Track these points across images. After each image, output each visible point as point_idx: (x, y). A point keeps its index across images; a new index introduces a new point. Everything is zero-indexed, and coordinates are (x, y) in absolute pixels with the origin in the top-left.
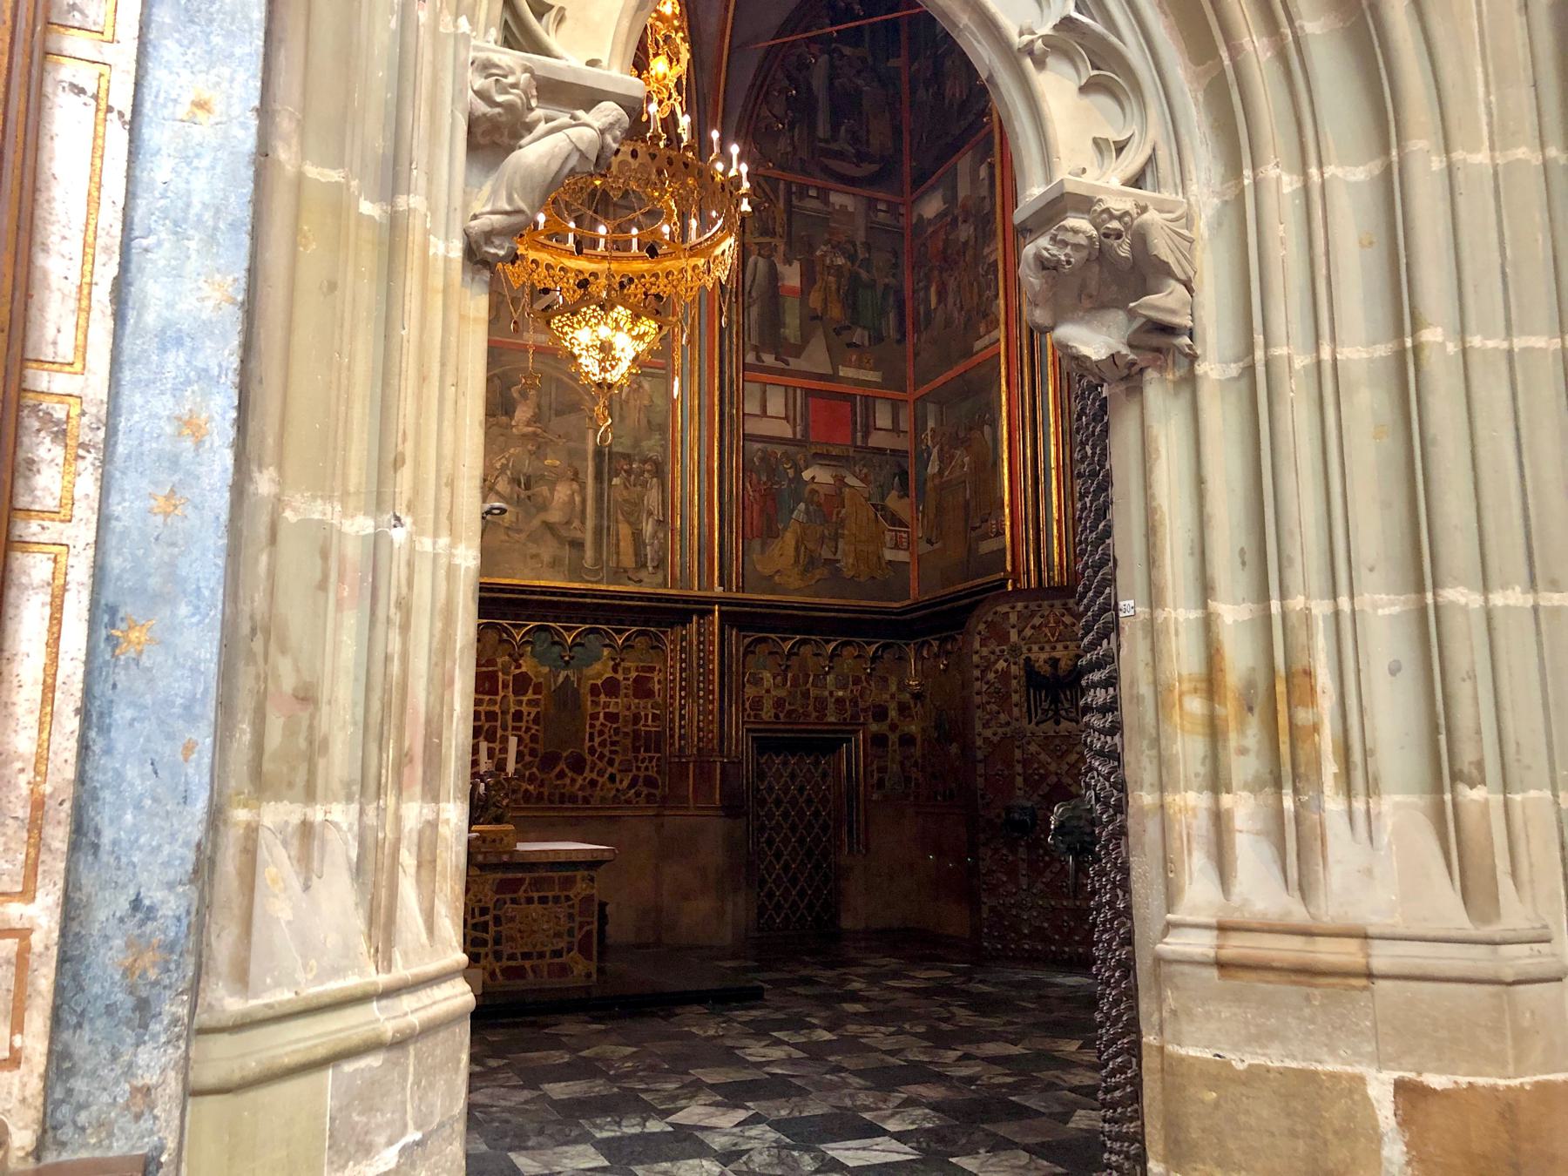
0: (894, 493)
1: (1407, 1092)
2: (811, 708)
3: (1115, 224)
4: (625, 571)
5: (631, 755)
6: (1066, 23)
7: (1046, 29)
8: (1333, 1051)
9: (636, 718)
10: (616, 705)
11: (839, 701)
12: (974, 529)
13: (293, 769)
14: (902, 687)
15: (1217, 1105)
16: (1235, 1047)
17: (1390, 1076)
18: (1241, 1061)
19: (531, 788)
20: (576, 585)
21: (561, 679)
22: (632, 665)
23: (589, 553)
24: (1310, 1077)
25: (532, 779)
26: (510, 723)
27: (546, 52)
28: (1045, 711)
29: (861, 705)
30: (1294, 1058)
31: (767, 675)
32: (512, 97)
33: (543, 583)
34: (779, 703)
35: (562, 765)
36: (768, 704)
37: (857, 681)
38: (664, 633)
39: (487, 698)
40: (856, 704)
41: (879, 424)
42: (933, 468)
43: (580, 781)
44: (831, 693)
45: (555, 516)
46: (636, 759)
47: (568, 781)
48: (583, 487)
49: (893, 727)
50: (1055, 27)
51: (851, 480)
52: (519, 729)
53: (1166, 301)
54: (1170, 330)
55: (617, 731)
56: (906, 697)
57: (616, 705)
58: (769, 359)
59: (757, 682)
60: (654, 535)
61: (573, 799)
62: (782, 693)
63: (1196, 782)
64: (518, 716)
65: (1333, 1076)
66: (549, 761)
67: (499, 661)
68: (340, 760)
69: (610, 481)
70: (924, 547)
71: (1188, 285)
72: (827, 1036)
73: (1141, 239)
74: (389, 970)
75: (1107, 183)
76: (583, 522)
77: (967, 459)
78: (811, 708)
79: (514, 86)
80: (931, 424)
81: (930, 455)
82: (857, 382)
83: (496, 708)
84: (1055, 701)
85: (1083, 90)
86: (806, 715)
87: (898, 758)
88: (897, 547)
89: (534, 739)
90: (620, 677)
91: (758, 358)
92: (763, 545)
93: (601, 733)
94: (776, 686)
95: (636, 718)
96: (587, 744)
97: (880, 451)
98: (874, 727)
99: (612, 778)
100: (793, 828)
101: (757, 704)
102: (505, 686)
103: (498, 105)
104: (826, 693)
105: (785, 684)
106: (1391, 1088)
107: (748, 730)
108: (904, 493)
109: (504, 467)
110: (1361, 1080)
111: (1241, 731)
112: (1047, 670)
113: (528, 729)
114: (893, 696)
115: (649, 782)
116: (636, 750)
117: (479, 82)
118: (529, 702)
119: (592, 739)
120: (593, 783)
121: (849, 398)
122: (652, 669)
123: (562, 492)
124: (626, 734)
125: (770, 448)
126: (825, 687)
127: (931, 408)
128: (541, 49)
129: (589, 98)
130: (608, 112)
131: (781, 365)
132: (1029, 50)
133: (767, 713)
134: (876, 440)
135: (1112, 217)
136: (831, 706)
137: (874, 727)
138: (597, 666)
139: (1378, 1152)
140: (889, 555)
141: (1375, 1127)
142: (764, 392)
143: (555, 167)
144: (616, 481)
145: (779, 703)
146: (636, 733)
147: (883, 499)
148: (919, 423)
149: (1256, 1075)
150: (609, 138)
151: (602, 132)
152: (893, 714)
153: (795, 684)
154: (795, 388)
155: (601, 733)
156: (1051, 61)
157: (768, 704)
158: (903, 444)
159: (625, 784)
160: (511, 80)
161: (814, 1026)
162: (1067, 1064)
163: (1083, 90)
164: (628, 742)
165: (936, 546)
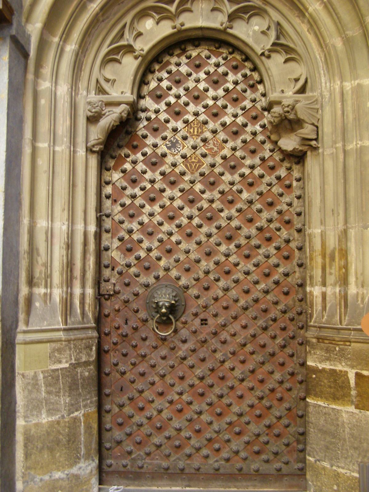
1: (358, 375)
3: (286, 109)
6: (274, 44)
7: (269, 47)
8: (341, 363)
13: (42, 281)
15: (315, 378)
16: (320, 362)
17: (354, 371)
18: (320, 366)
24: (334, 371)
27: (108, 94)
30: (331, 365)
32: (97, 109)
50: (271, 46)
53: (307, 131)
63: (319, 283)
65: (341, 371)
68: (57, 278)
71: (313, 124)
74: (67, 325)
79: (97, 106)
85: (286, 61)
106: (354, 375)
110: (346, 372)
111: (331, 268)
117: (89, 107)
129: (118, 104)
130: (123, 107)
132: (263, 54)
135: (286, 107)
139: (350, 393)
141: (350, 386)
143: (107, 126)
149: (324, 369)
150: (123, 114)
151: (121, 113)
160: (96, 105)
163: (286, 61)
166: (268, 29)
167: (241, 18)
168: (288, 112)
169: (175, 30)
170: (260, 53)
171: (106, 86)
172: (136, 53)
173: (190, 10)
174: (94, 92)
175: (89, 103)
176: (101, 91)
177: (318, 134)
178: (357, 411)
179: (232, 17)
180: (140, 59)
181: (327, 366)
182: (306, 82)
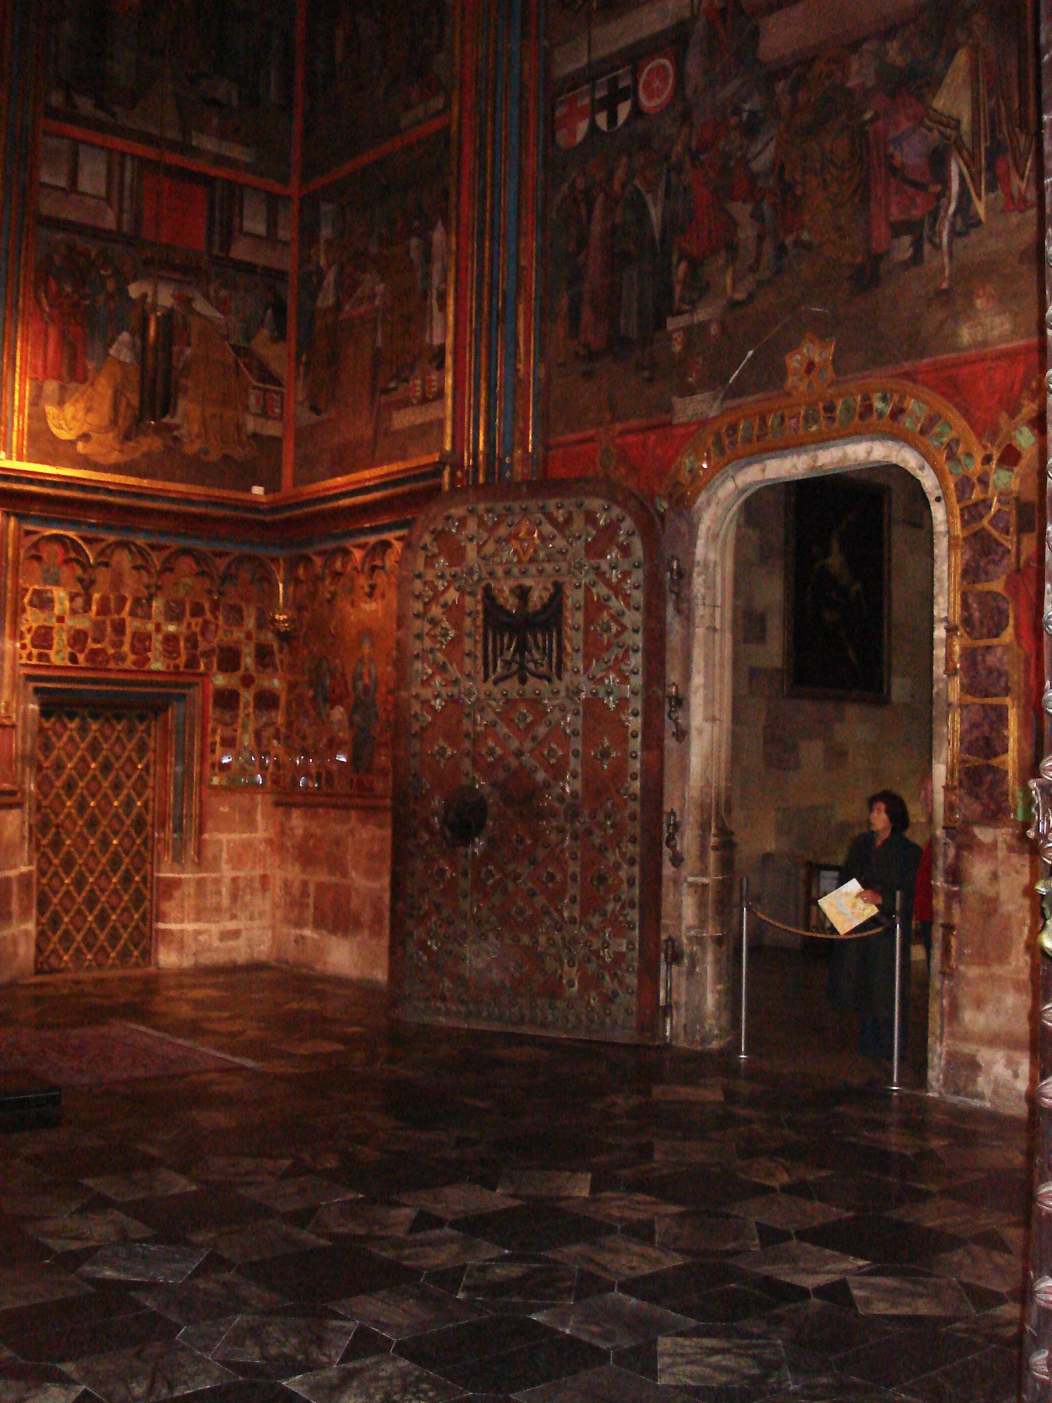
0: (265, 332)
2: (126, 648)
11: (170, 639)
12: (386, 391)
14: (264, 621)
28: (507, 664)
29: (202, 646)
31: (60, 595)
34: (78, 638)
36: (60, 640)
37: (197, 611)
40: (195, 646)
41: (248, 225)
42: (326, 299)
44: (158, 628)
49: (247, 681)
51: (201, 306)
56: (269, 637)
58: (85, 105)
59: (43, 602)
62: (82, 623)
70: (306, 417)
72: (182, 1185)
77: (380, 288)
78: (126, 648)
80: (326, 232)
81: (321, 281)
82: (220, 160)
84: (522, 648)
86: (121, 658)
87: (251, 728)
88: (265, 414)
91: (69, 99)
92: (63, 389)
94: (73, 612)
97: (250, 268)
98: (220, 680)
100: (92, 824)
101: (43, 638)
104: (151, 627)
105: (87, 607)
107: (29, 678)
108: (280, 334)
112: (510, 602)
114: (249, 636)
121: (209, 181)
125: (80, 242)
126: (148, 617)
127: (326, 208)
131: (102, 115)
134: (241, 251)
136: (157, 642)
137: (220, 680)
140: (251, 424)
142: (76, 154)
145: (78, 638)
147: (248, 339)
148: (308, 233)
152: (248, 661)
153: (104, 609)
154: (123, 155)
157: (60, 640)
158: (286, 261)
161: (151, 1163)
162: (588, 1229)
165: (324, 416)
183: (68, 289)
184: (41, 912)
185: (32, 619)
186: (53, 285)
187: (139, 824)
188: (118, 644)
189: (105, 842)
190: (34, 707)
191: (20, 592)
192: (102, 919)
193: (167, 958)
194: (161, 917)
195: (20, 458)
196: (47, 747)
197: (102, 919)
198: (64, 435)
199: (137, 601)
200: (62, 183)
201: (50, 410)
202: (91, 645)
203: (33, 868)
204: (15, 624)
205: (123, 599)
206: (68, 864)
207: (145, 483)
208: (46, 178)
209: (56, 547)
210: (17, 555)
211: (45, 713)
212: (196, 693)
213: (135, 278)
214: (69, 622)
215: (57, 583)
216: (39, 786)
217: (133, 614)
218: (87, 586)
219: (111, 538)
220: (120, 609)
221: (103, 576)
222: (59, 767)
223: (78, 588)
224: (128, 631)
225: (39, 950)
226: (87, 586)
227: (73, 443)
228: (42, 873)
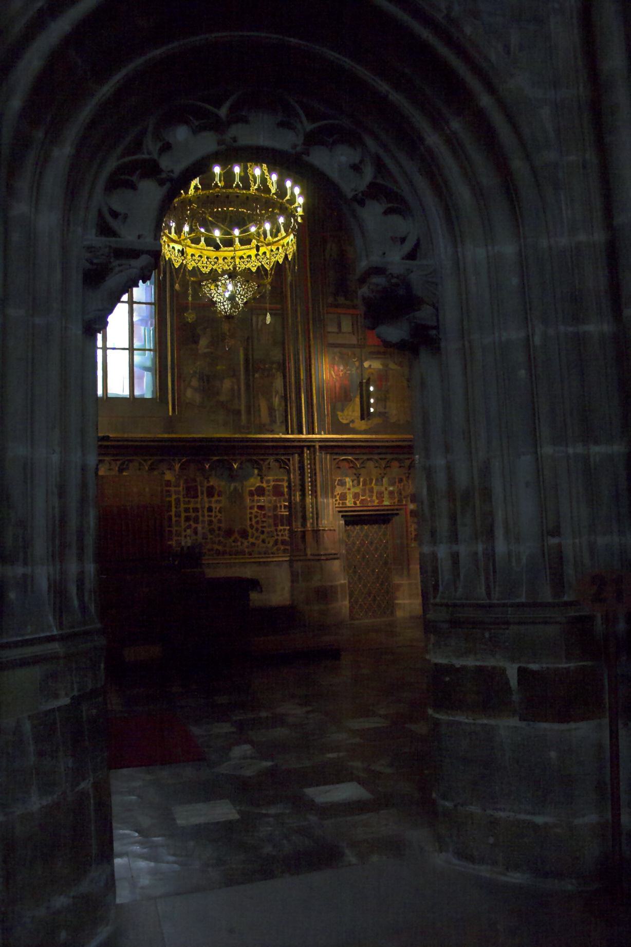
1: (521, 671)
2: (374, 498)
4: (264, 425)
5: (273, 529)
6: (372, 185)
9: (275, 508)
10: (263, 501)
11: (391, 493)
17: (516, 666)
18: (458, 663)
19: (220, 548)
20: (236, 436)
21: (232, 488)
22: (270, 478)
23: (244, 417)
25: (220, 543)
26: (206, 514)
30: (478, 660)
31: (348, 480)
33: (218, 436)
34: (356, 496)
35: (236, 535)
38: (289, 460)
39: (193, 500)
43: (246, 544)
45: (223, 398)
46: (276, 530)
47: (239, 544)
48: (238, 380)
52: (211, 516)
53: (424, 314)
54: (426, 328)
55: (264, 515)
57: (263, 501)
58: (341, 300)
59: (342, 484)
60: (280, 404)
61: (243, 553)
62: (357, 490)
64: (210, 509)
65: (494, 668)
66: (229, 533)
67: (198, 479)
68: (40, 547)
69: (253, 375)
73: (408, 286)
75: (395, 259)
76: (239, 398)
83: (199, 506)
85: (386, 213)
86: (372, 501)
89: (220, 521)
90: (264, 485)
93: (256, 517)
94: (353, 486)
95: (275, 508)
96: (249, 522)
99: (263, 541)
101: (343, 497)
102: (202, 494)
103: (96, 264)
104: (383, 489)
107: (340, 512)
109: (195, 372)
110: (504, 671)
113: (216, 516)
115: (283, 542)
116: (276, 525)
118: (217, 501)
119: (251, 519)
120: (253, 544)
122: (283, 480)
123: (227, 384)
124: (269, 517)
128: (114, 234)
131: (348, 302)
132: (355, 199)
133: (349, 502)
136: (386, 495)
138: (252, 480)
144: (257, 375)
146: (276, 516)
149: (464, 668)
155: (256, 517)
156: (367, 202)
159: (271, 544)
163: (386, 213)
164: (271, 521)
166: (361, 162)
167: (322, 143)
168: (397, 285)
169: (223, 147)
170: (350, 195)
171: (114, 224)
172: (164, 176)
173: (245, 121)
174: (94, 231)
175: (90, 248)
176: (105, 230)
177: (438, 320)
178: (523, 724)
179: (312, 139)
180: (168, 185)
181: (470, 662)
182: (417, 245)
183: (342, 368)
184: (351, 597)
185: (339, 490)
186: (336, 368)
187: (386, 563)
188: (371, 496)
189: (373, 571)
190: (342, 522)
191: (333, 481)
192: (374, 600)
193: (399, 614)
194: (396, 598)
195: (329, 434)
196: (349, 536)
197: (374, 600)
198: (344, 422)
199: (377, 480)
200: (336, 330)
201: (339, 413)
202: (361, 498)
203: (346, 581)
204: (332, 493)
205: (371, 480)
206: (360, 578)
207: (374, 436)
208: (330, 330)
209: (345, 463)
210: (331, 469)
211: (347, 523)
212: (402, 512)
213: (366, 360)
214: (352, 490)
215: (346, 476)
216: (347, 550)
217: (376, 484)
218: (358, 476)
219: (365, 457)
220: (371, 483)
221: (363, 471)
222: (354, 544)
223: (355, 477)
224: (375, 491)
225: (351, 611)
226: (358, 476)
227: (348, 424)
228: (349, 582)
